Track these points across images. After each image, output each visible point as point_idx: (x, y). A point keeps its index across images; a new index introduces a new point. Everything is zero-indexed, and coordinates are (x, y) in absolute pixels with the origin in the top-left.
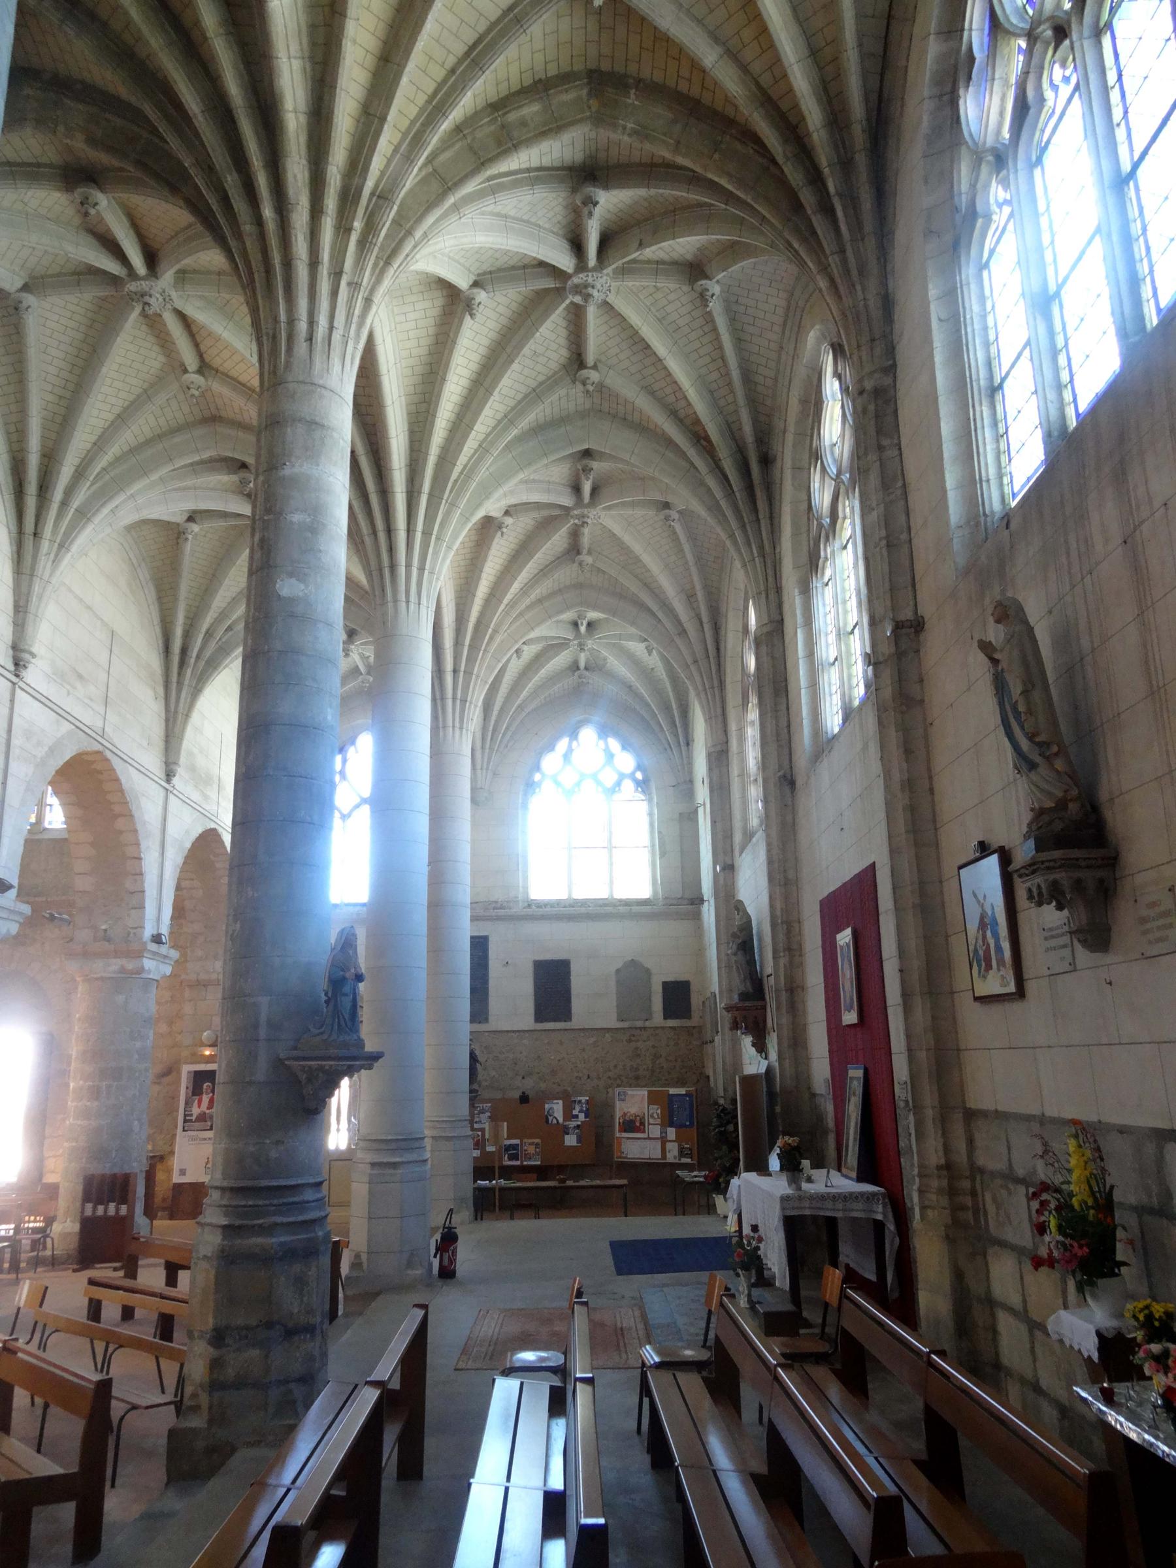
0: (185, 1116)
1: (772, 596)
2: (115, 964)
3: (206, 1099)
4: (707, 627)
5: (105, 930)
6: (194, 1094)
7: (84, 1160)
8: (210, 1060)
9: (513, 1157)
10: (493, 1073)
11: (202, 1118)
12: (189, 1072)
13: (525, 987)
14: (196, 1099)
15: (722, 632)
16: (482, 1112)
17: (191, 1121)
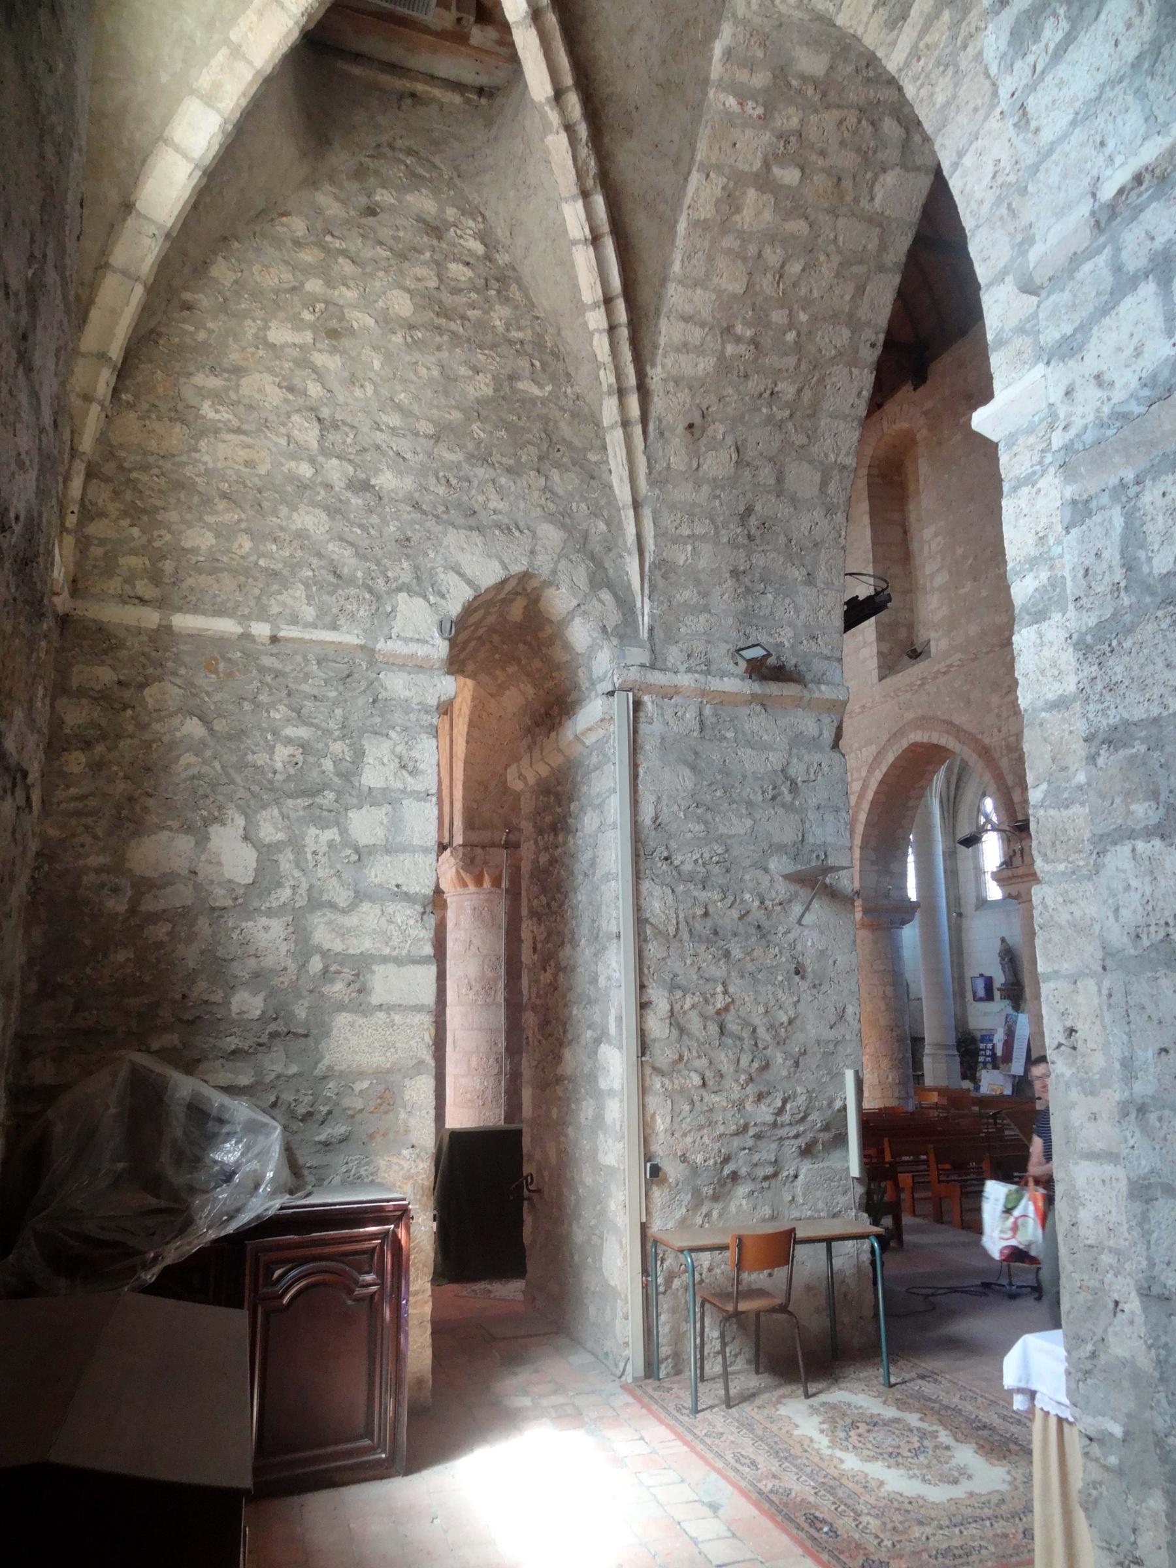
4: (953, 787)
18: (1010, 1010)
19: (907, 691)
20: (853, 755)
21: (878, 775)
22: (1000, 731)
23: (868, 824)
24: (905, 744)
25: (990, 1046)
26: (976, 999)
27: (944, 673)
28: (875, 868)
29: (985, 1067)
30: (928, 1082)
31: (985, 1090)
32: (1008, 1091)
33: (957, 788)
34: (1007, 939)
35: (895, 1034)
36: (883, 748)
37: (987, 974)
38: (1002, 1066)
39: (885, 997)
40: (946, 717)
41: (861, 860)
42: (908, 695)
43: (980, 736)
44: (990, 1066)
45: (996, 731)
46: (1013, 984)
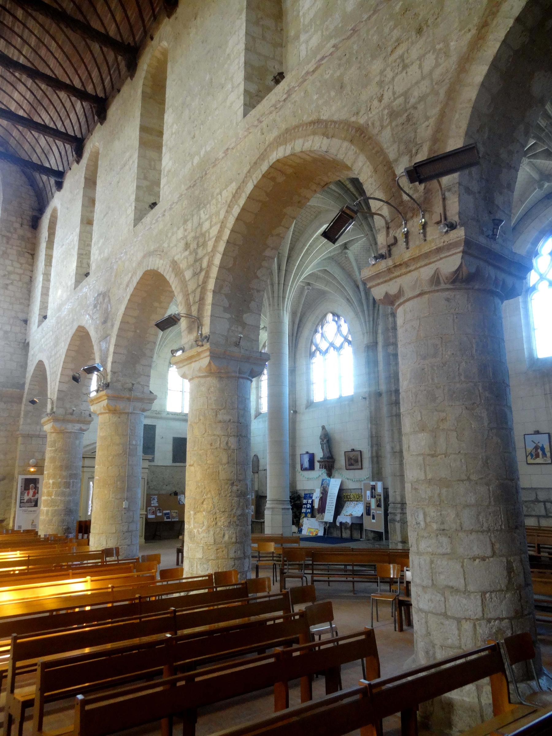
0: (21, 500)
1: (375, 334)
2: (77, 426)
3: (31, 492)
5: (74, 410)
6: (25, 489)
7: (62, 516)
8: (33, 473)
9: (168, 518)
10: (155, 483)
11: (29, 501)
12: (22, 479)
13: (169, 448)
14: (27, 492)
15: (301, 329)
16: (154, 499)
17: (23, 502)
18: (325, 476)
19: (271, 113)
20: (214, 201)
21: (236, 211)
22: (380, 101)
23: (221, 267)
24: (265, 167)
25: (310, 501)
26: (303, 469)
27: (314, 71)
28: (228, 316)
29: (306, 516)
30: (268, 531)
31: (305, 532)
32: (321, 533)
33: (299, 327)
34: (326, 427)
35: (235, 488)
36: (243, 182)
37: (311, 452)
38: (318, 516)
39: (227, 449)
40: (314, 117)
41: (213, 304)
42: (271, 117)
43: (353, 119)
44: (309, 515)
45: (376, 103)
46: (328, 458)
